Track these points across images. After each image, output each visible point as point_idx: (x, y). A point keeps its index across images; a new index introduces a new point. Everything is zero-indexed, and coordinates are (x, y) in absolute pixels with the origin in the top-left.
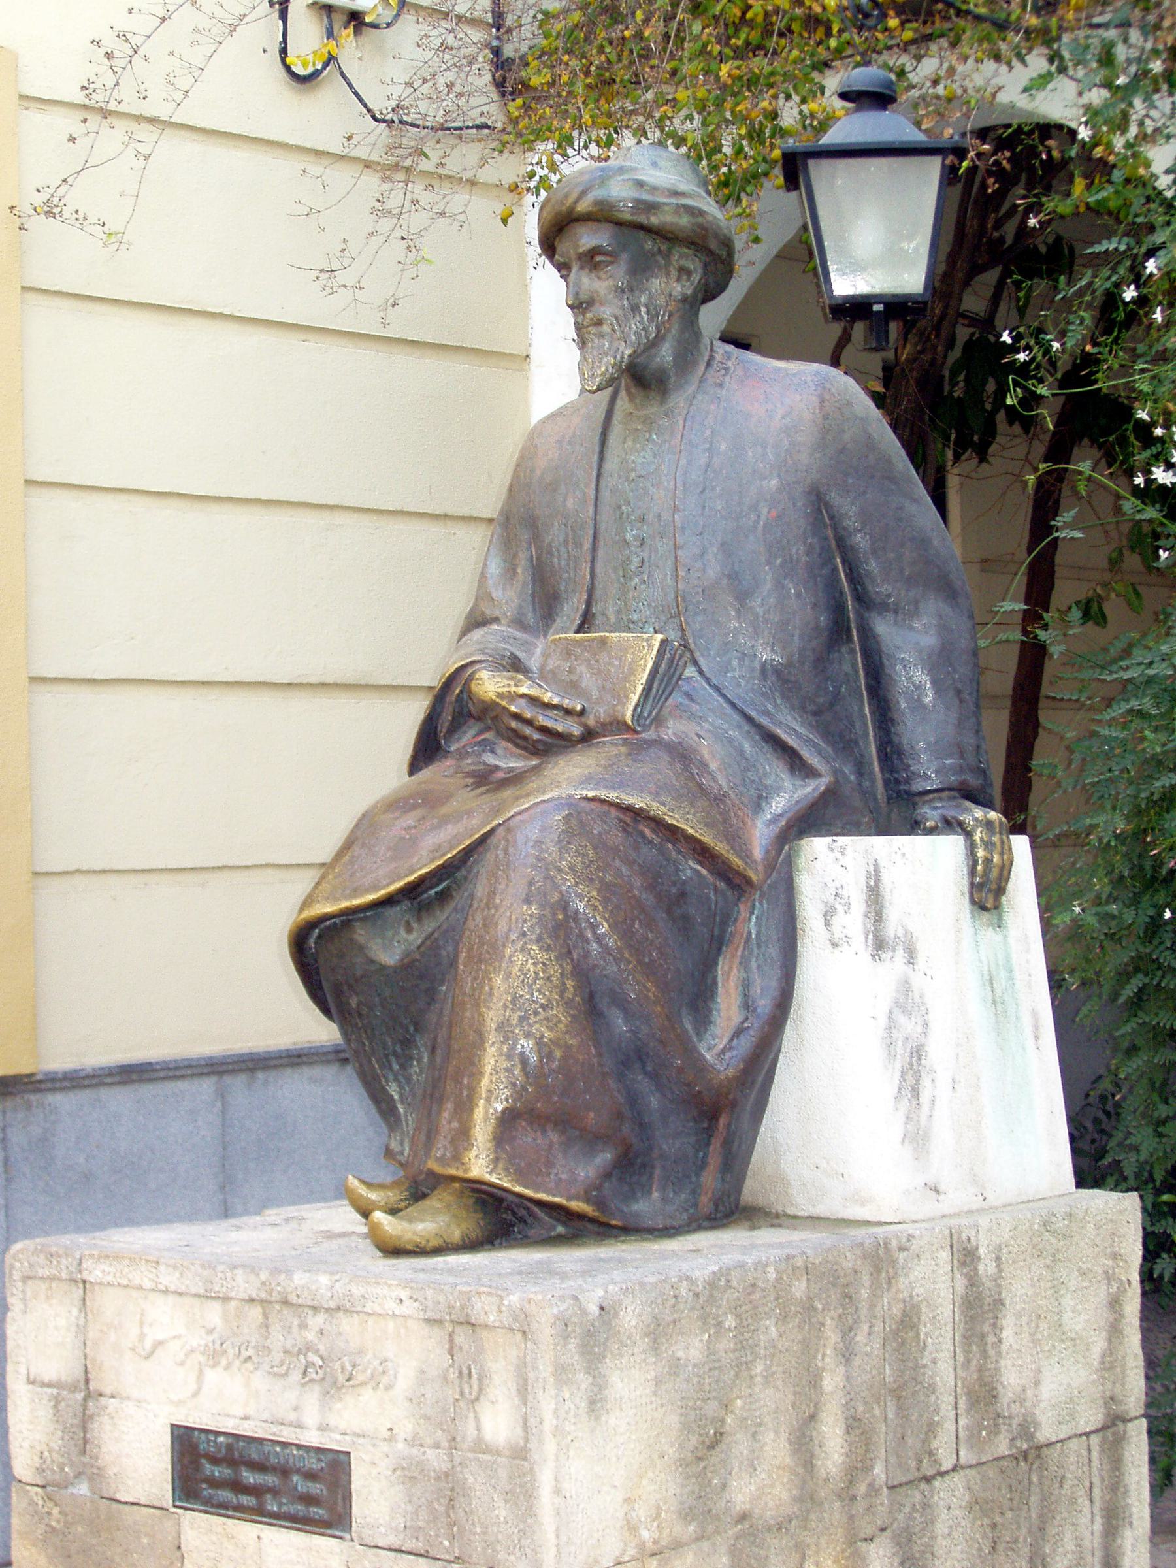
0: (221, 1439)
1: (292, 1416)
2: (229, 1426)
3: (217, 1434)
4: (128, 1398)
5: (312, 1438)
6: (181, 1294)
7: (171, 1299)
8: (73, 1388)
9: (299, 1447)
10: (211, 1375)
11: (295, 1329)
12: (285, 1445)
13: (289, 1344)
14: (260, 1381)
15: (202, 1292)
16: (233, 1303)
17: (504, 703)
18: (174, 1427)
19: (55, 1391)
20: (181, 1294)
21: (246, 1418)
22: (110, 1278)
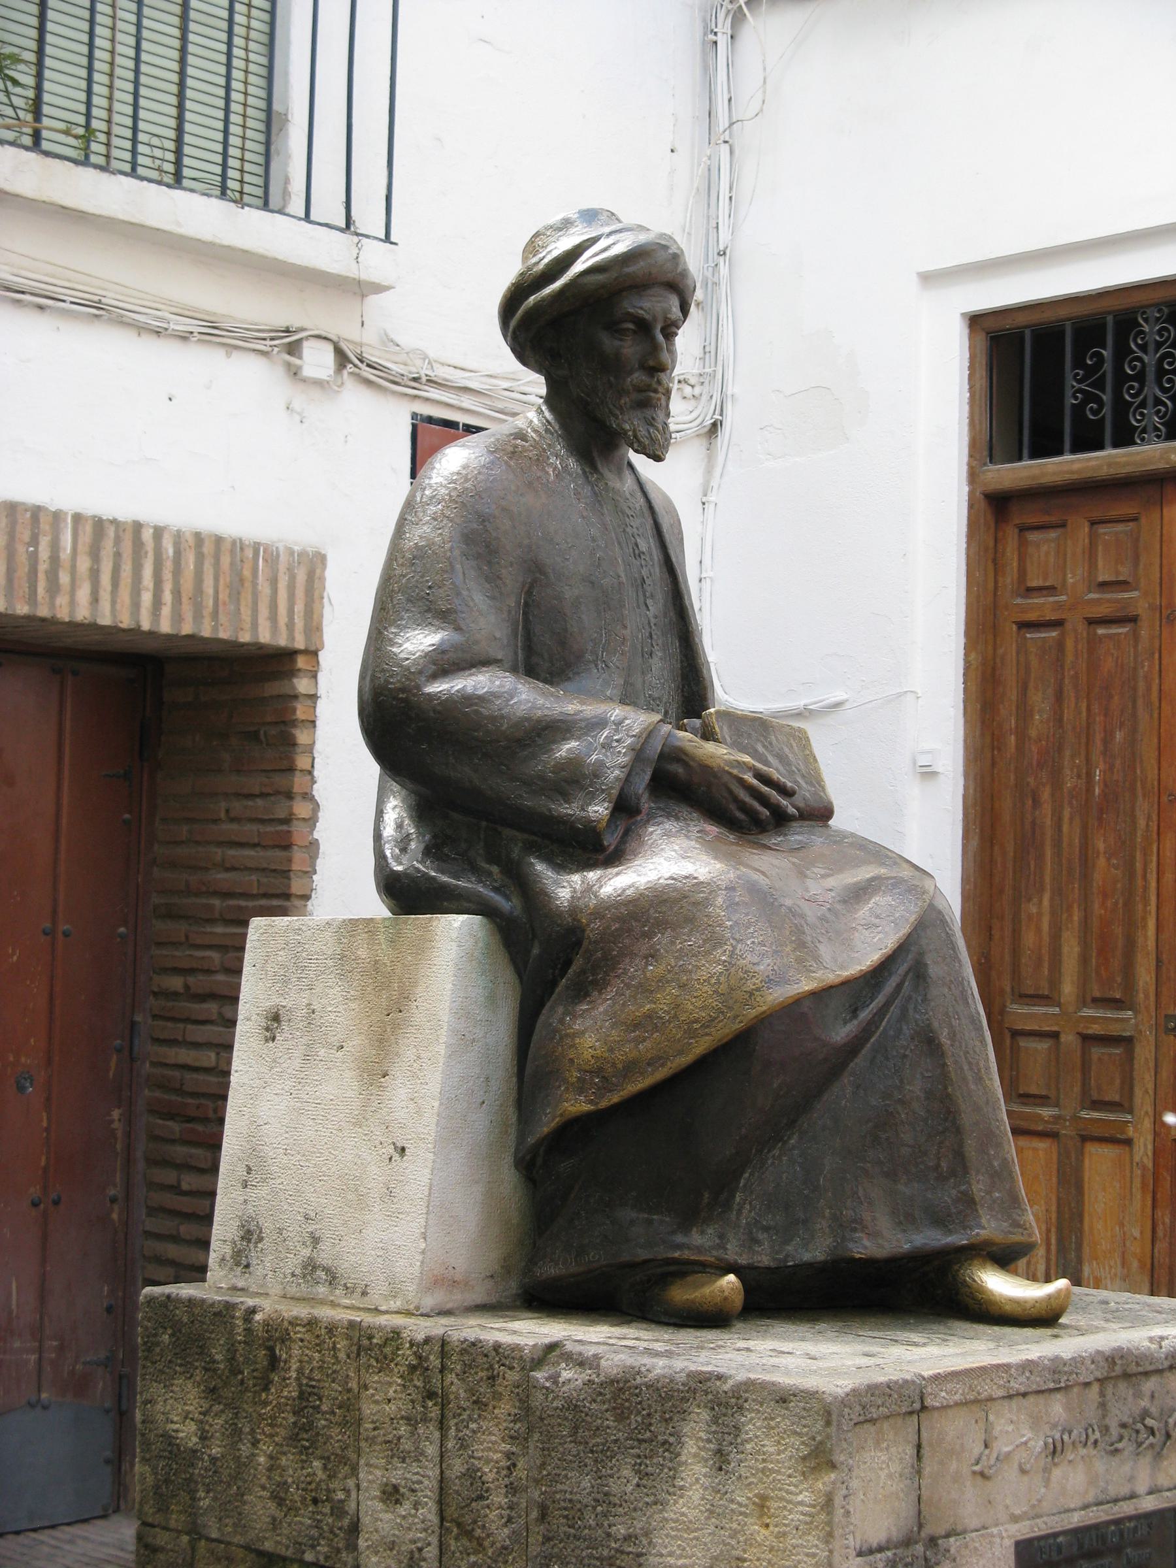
0: (1060, 1539)
1: (1125, 1490)
2: (1076, 1519)
3: (1055, 1535)
4: (964, 1532)
5: (1149, 1504)
6: (1024, 1395)
7: (1014, 1403)
8: (907, 1542)
9: (1130, 1518)
10: (1057, 1473)
11: (1130, 1399)
12: (1117, 1522)
13: (1125, 1419)
14: (1100, 1466)
15: (1052, 1385)
16: (1075, 1390)
17: (735, 772)
18: (1018, 1544)
19: (889, 1554)
20: (1024, 1395)
21: (1085, 1507)
22: (957, 1397)
